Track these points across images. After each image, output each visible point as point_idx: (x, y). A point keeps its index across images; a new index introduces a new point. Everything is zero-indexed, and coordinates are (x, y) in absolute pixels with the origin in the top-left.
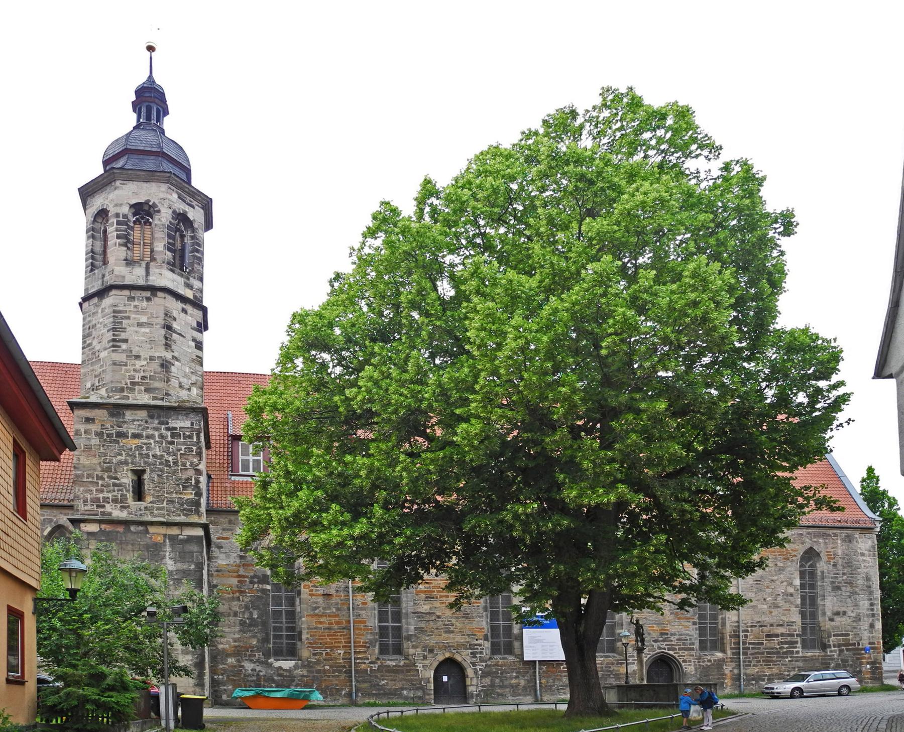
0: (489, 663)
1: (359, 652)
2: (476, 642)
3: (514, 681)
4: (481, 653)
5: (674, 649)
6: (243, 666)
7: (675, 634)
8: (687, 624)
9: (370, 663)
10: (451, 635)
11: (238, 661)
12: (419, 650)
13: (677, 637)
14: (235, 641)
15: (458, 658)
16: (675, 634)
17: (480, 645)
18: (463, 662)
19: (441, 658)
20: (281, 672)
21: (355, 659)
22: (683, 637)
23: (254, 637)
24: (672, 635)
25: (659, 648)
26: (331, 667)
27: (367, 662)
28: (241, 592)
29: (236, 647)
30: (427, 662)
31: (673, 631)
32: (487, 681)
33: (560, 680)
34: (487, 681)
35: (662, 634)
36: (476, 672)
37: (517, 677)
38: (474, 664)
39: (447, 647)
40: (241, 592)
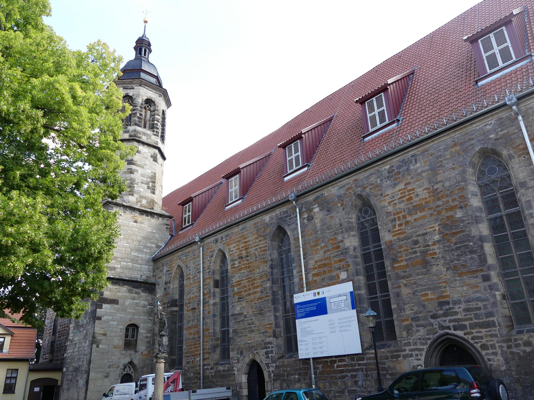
2: (268, 340)
5: (463, 328)
7: (459, 302)
8: (473, 281)
9: (212, 369)
10: (252, 335)
12: (235, 352)
13: (463, 306)
16: (459, 302)
17: (270, 343)
19: (247, 360)
21: (204, 366)
22: (473, 305)
24: (455, 303)
25: (442, 328)
30: (239, 365)
31: (456, 296)
33: (336, 384)
35: (441, 304)
36: (270, 376)
39: (251, 348)
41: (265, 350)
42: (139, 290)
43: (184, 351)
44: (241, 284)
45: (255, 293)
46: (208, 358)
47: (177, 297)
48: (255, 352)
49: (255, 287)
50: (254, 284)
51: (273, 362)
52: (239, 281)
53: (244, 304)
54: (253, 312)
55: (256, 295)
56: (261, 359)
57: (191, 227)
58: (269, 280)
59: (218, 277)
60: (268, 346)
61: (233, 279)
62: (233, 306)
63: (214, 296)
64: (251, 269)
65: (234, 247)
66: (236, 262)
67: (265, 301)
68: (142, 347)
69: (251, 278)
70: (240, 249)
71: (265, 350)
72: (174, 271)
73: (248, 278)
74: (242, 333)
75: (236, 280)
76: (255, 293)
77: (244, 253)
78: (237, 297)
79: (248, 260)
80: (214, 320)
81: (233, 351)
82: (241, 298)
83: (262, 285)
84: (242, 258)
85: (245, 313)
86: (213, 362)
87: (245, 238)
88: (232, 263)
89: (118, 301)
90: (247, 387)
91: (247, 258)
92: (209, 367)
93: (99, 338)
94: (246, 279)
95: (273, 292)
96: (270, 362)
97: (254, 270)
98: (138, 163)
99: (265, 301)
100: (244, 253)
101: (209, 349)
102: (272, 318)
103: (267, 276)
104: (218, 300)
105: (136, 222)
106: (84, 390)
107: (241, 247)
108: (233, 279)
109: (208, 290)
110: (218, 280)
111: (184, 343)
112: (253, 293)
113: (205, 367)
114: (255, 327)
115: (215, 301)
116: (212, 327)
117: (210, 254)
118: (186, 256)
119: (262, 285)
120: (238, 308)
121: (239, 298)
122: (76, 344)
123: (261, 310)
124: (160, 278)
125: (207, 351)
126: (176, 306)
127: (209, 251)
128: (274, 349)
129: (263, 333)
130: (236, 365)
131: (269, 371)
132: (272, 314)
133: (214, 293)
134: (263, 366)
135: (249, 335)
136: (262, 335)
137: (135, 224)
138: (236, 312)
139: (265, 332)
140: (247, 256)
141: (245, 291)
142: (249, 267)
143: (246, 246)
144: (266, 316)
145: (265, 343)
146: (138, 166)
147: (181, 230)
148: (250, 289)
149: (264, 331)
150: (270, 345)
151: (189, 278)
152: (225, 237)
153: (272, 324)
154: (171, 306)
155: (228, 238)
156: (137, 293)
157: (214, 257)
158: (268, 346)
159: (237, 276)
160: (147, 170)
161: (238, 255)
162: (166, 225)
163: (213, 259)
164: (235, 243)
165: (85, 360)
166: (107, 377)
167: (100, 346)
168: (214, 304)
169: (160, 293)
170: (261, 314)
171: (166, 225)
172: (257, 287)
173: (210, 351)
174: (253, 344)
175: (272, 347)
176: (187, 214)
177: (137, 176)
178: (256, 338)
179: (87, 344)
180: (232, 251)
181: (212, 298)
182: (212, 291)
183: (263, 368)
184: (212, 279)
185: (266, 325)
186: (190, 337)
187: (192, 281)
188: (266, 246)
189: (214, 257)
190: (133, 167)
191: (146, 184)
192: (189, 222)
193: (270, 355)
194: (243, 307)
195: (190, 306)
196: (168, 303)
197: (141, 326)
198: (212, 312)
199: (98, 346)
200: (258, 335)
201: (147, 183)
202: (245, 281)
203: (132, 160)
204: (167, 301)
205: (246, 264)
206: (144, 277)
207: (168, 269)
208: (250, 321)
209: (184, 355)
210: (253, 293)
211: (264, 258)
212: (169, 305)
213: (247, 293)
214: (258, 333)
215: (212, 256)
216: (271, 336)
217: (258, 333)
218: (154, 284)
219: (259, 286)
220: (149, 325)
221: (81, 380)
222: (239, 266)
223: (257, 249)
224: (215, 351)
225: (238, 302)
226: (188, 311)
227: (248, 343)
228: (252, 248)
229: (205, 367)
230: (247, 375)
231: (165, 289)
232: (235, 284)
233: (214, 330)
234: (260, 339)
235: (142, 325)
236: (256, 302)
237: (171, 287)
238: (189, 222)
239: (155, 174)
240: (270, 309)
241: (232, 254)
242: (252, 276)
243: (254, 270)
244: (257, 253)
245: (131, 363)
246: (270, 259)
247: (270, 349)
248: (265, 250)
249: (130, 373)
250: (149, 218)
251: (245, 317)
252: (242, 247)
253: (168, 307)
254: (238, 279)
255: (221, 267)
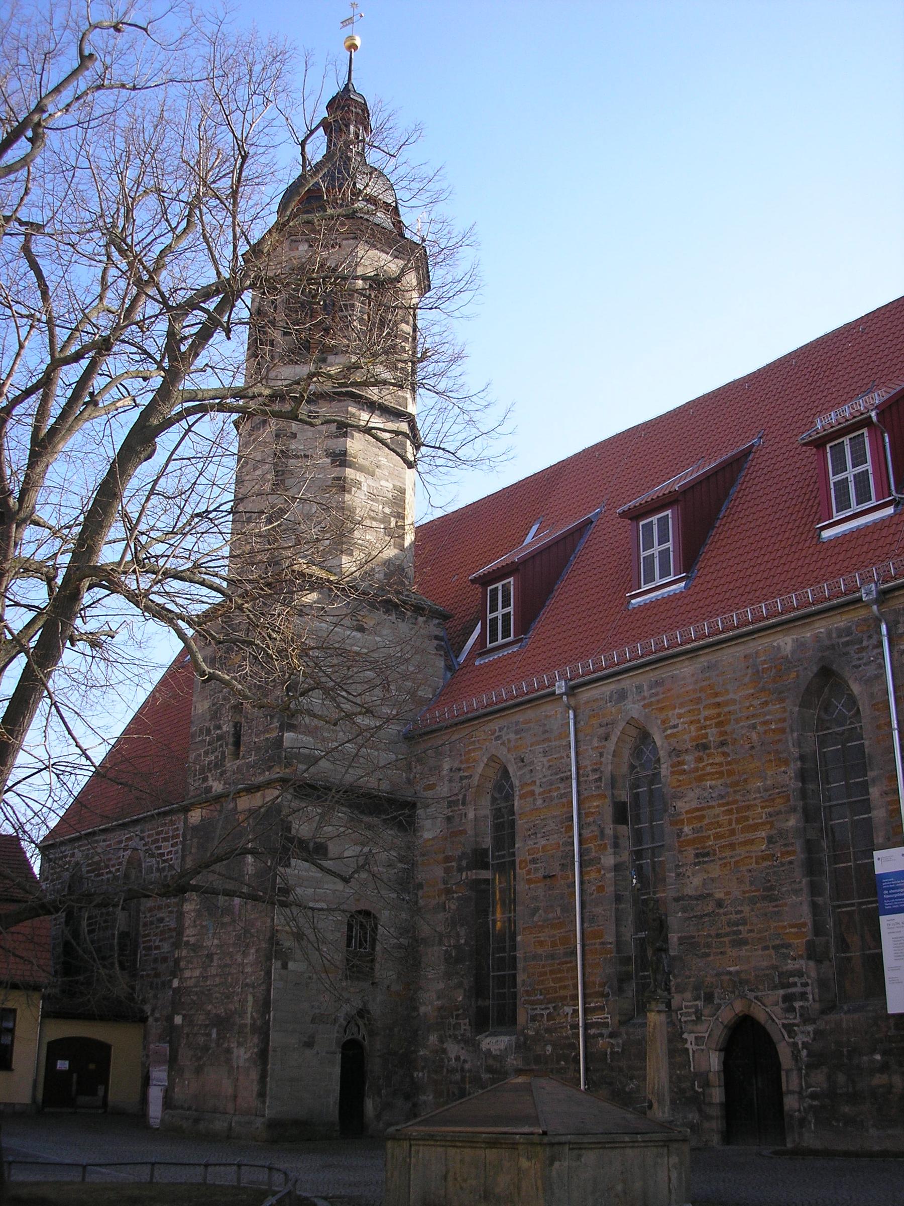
0: (821, 1025)
1: (595, 1009)
2: (791, 965)
3: (879, 1079)
4: (803, 996)
6: (444, 1051)
9: (612, 1035)
10: (744, 952)
11: (442, 1040)
12: (688, 995)
14: (438, 998)
15: (761, 1017)
17: (800, 973)
18: (770, 1028)
19: (727, 1015)
20: (491, 1062)
23: (460, 985)
26: (554, 1046)
27: (606, 1032)
28: (448, 891)
29: (440, 1009)
30: (702, 1029)
32: (819, 1078)
34: (819, 1078)
36: (796, 1057)
37: (884, 1068)
38: (789, 1028)
40: (448, 891)
41: (782, 992)
42: (373, 820)
43: (520, 989)
44: (703, 817)
45: (752, 842)
46: (602, 1008)
47: (488, 842)
48: (751, 995)
49: (751, 826)
50: (746, 818)
51: (806, 1020)
52: (698, 809)
53: (715, 871)
54: (744, 892)
55: (754, 848)
56: (769, 1010)
57: (515, 648)
58: (794, 810)
59: (624, 796)
60: (791, 980)
61: (679, 804)
62: (678, 875)
63: (616, 845)
64: (735, 778)
65: (680, 716)
66: (688, 758)
67: (782, 864)
68: (386, 971)
69: (735, 802)
70: (699, 721)
71: (782, 992)
72: (480, 770)
73: (728, 804)
74: (708, 945)
75: (687, 807)
76: (752, 842)
77: (712, 735)
78: (690, 852)
79: (725, 754)
80: (617, 909)
81: (681, 989)
82: (707, 854)
83: (771, 823)
84: (705, 747)
85: (719, 895)
86: (617, 1018)
87: (716, 695)
88: (675, 759)
89: (326, 849)
90: (722, 1083)
91: (725, 749)
92: (606, 1032)
93: (288, 943)
94: (719, 805)
95: (808, 842)
96: (796, 1021)
97: (746, 781)
98: (361, 461)
99: (782, 864)
100: (712, 735)
101: (603, 985)
102: (806, 909)
103: (789, 800)
104: (625, 856)
105: (361, 629)
106: (254, 1075)
107: (701, 717)
108: (679, 804)
109: (595, 828)
110: (625, 803)
111: (520, 965)
112: (745, 843)
113: (592, 1032)
114: (751, 931)
115: (619, 859)
116: (613, 927)
117: (602, 731)
118: (517, 733)
119: (771, 823)
120: (697, 881)
121: (697, 856)
122: (210, 956)
123: (771, 888)
124: (431, 787)
125: (597, 989)
126: (485, 866)
127: (595, 722)
128: (809, 989)
129: (773, 947)
130: (690, 1027)
131: (795, 1044)
132: (804, 899)
133: (616, 837)
134: (775, 1031)
135: (732, 952)
136: (772, 951)
137: (358, 635)
138: (689, 891)
139: (782, 946)
140: (723, 744)
141: (718, 837)
142: (730, 773)
143: (719, 715)
144: (786, 904)
145: (781, 975)
146: (360, 469)
147: (480, 655)
148: (732, 832)
149: (778, 942)
150: (796, 979)
151: (532, 793)
152: (651, 688)
153: (804, 925)
154: (469, 868)
155: (659, 689)
156: (369, 827)
157: (614, 739)
158: (791, 980)
159: (691, 795)
160: (383, 483)
161: (692, 740)
162: (436, 638)
163: (611, 745)
164: (682, 705)
165: (250, 998)
166: (309, 1044)
167: (291, 965)
168: (617, 868)
169: (430, 829)
170: (771, 899)
171: (436, 638)
172: (755, 827)
173: (607, 990)
174: (743, 976)
175: (805, 985)
176: (500, 612)
177: (358, 499)
178: (753, 960)
179: (251, 958)
180: (675, 726)
181: (610, 850)
182: (609, 831)
183: (775, 1037)
184: (608, 801)
185: (785, 927)
186: (540, 951)
187: (539, 802)
188: (784, 720)
189: (614, 739)
190: (349, 472)
191: (382, 522)
192: (506, 634)
193: (797, 1005)
194: (713, 880)
195: (536, 870)
196: (460, 858)
197: (385, 916)
198: (610, 890)
199: (285, 966)
200: (760, 952)
201: (385, 520)
202: (717, 811)
203: (344, 453)
204: (459, 852)
205: (721, 764)
206: (385, 786)
207: (456, 765)
208: (734, 917)
209: (521, 999)
210: (745, 843)
211: (777, 752)
212: (464, 863)
213: (723, 842)
214: (760, 946)
215: (607, 738)
216: (801, 957)
217: (760, 946)
218: (413, 806)
219: (762, 824)
220: (404, 916)
221: (242, 1051)
222: (696, 769)
223: (754, 727)
224: (621, 990)
225: (695, 864)
226: (529, 881)
227: (730, 973)
228: (737, 721)
229: (592, 1032)
230: (723, 1054)
231: (449, 819)
232: (684, 816)
233: (618, 935)
234: (765, 964)
235: (387, 913)
236: (754, 865)
237: (471, 815)
238: (506, 634)
239: (403, 492)
240: (796, 886)
241: (672, 735)
242: (738, 797)
243: (746, 781)
244: (754, 736)
245: (362, 1013)
246: (797, 755)
247: (797, 990)
248: (782, 731)
249: (360, 1037)
250: (393, 617)
251: (720, 904)
252: (706, 719)
253: (460, 870)
254: (694, 804)
255: (632, 767)
